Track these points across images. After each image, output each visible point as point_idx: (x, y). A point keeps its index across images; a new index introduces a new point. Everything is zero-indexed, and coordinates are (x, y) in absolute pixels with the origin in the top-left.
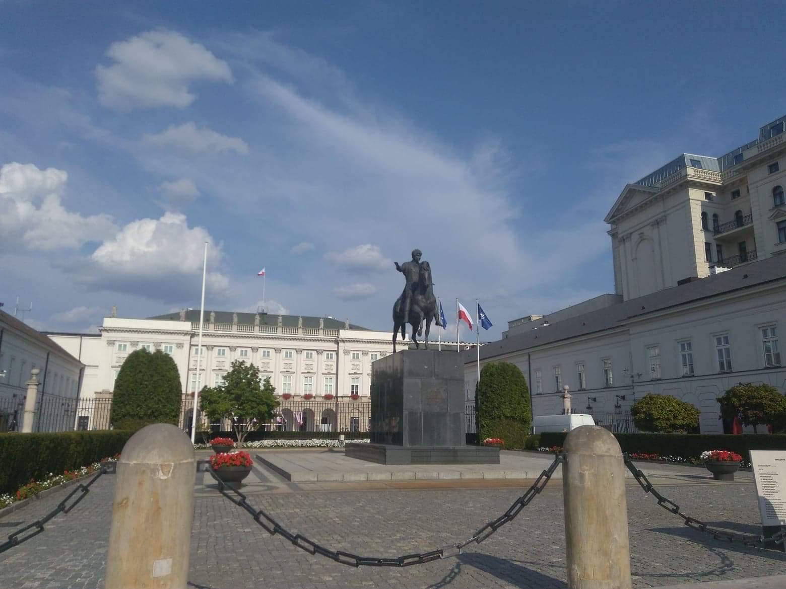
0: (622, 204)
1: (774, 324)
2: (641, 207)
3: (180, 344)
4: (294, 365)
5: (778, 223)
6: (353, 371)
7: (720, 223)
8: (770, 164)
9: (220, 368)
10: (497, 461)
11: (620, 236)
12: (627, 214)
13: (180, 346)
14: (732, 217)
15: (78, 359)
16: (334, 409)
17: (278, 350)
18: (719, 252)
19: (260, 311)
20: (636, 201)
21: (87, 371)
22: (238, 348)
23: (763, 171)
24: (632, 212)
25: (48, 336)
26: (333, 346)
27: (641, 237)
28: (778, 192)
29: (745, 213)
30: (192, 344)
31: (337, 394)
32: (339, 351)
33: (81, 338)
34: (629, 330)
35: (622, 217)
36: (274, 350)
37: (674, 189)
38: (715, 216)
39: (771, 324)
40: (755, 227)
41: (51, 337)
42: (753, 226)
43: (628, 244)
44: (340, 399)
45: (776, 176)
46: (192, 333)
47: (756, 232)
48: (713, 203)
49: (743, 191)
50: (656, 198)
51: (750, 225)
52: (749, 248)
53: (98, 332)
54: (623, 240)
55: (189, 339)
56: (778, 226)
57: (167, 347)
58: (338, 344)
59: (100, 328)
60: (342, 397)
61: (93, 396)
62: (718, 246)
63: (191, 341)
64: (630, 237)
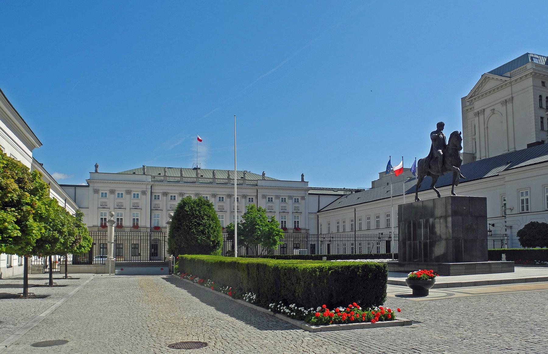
0: (478, 88)
10: (513, 271)
11: (476, 111)
13: (144, 193)
43: (481, 117)
50: (506, 85)
57: (135, 194)
63: (151, 190)
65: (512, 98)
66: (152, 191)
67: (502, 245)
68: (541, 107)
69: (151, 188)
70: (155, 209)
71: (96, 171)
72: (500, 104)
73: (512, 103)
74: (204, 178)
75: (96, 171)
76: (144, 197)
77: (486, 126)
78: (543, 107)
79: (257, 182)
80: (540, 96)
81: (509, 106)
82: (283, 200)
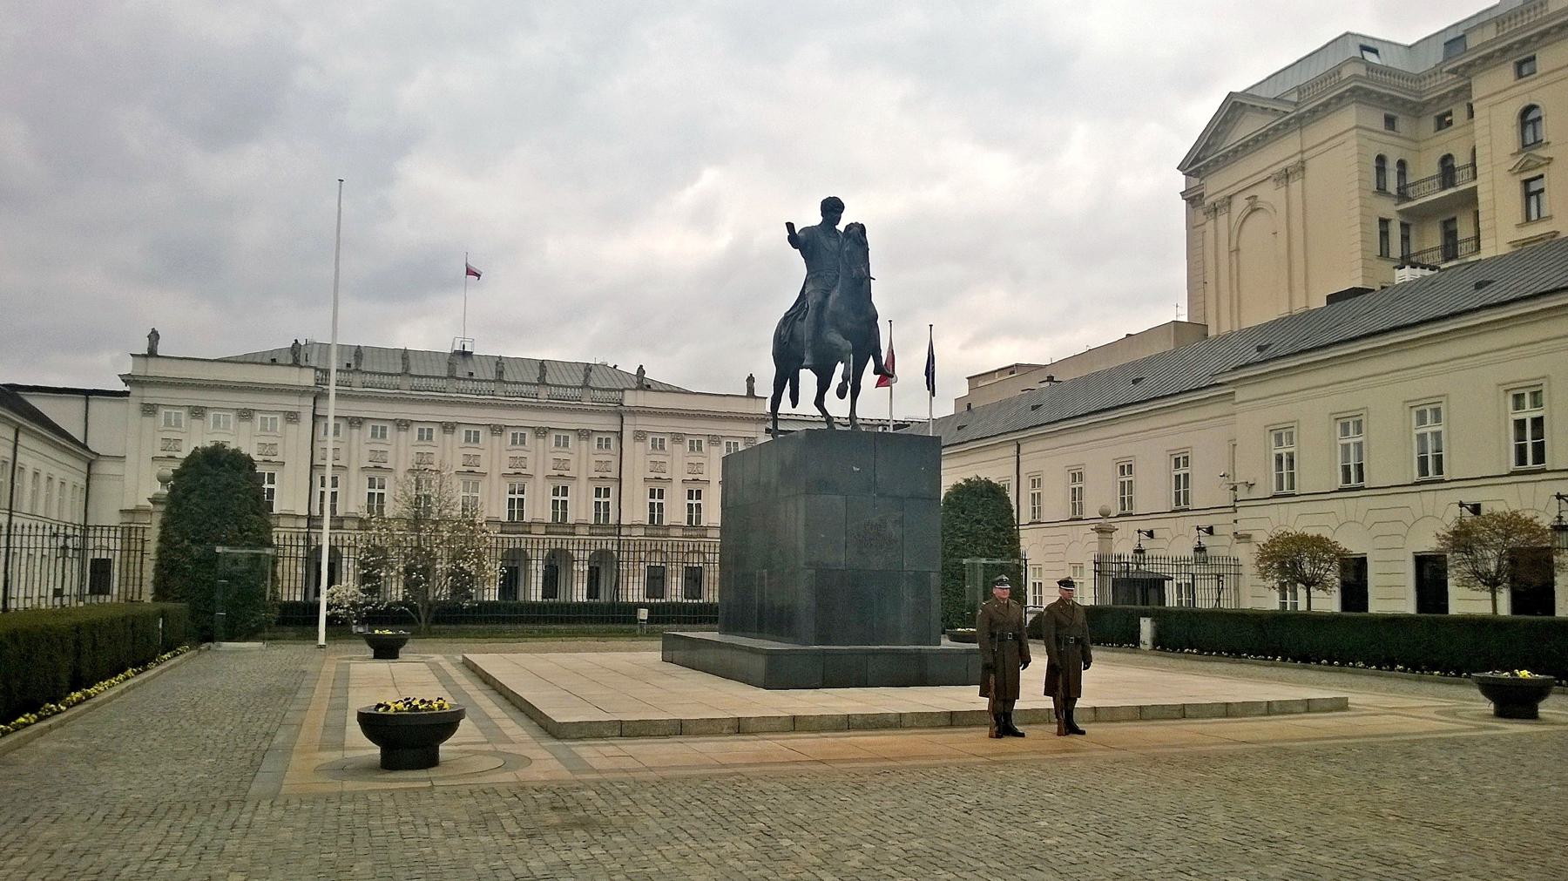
1: (1537, 382)
2: (1256, 140)
3: (290, 412)
4: (530, 463)
5: (1527, 182)
6: (653, 475)
7: (1410, 180)
9: (377, 464)
11: (1207, 202)
12: (1225, 156)
13: (292, 417)
14: (1434, 169)
15: (80, 438)
17: (497, 430)
18: (1405, 238)
19: (458, 348)
20: (1248, 127)
21: (104, 468)
22: (414, 424)
24: (1235, 151)
26: (610, 423)
27: (1250, 204)
28: (1531, 116)
29: (1461, 160)
30: (317, 413)
31: (620, 521)
32: (624, 432)
33: (87, 399)
34: (1234, 392)
35: (1216, 161)
36: (489, 432)
37: (1326, 105)
38: (1402, 164)
39: (1533, 383)
42: (1476, 187)
44: (624, 532)
45: (1530, 84)
46: (316, 390)
48: (1399, 137)
49: (1459, 114)
50: (1287, 124)
51: (1472, 184)
52: (1464, 230)
53: (121, 387)
54: (1215, 210)
55: (312, 404)
59: (126, 378)
60: (630, 526)
61: (115, 520)
62: (1402, 225)
63: (315, 408)
64: (1230, 204)
65: (1303, 162)
67: (1219, 594)
68: (1381, 190)
69: (315, 403)
71: (152, 353)
72: (1270, 182)
73: (1303, 178)
74: (476, 380)
75: (152, 353)
76: (292, 428)
78: (1388, 190)
79: (623, 395)
80: (1381, 160)
81: (1296, 185)
82: (696, 447)
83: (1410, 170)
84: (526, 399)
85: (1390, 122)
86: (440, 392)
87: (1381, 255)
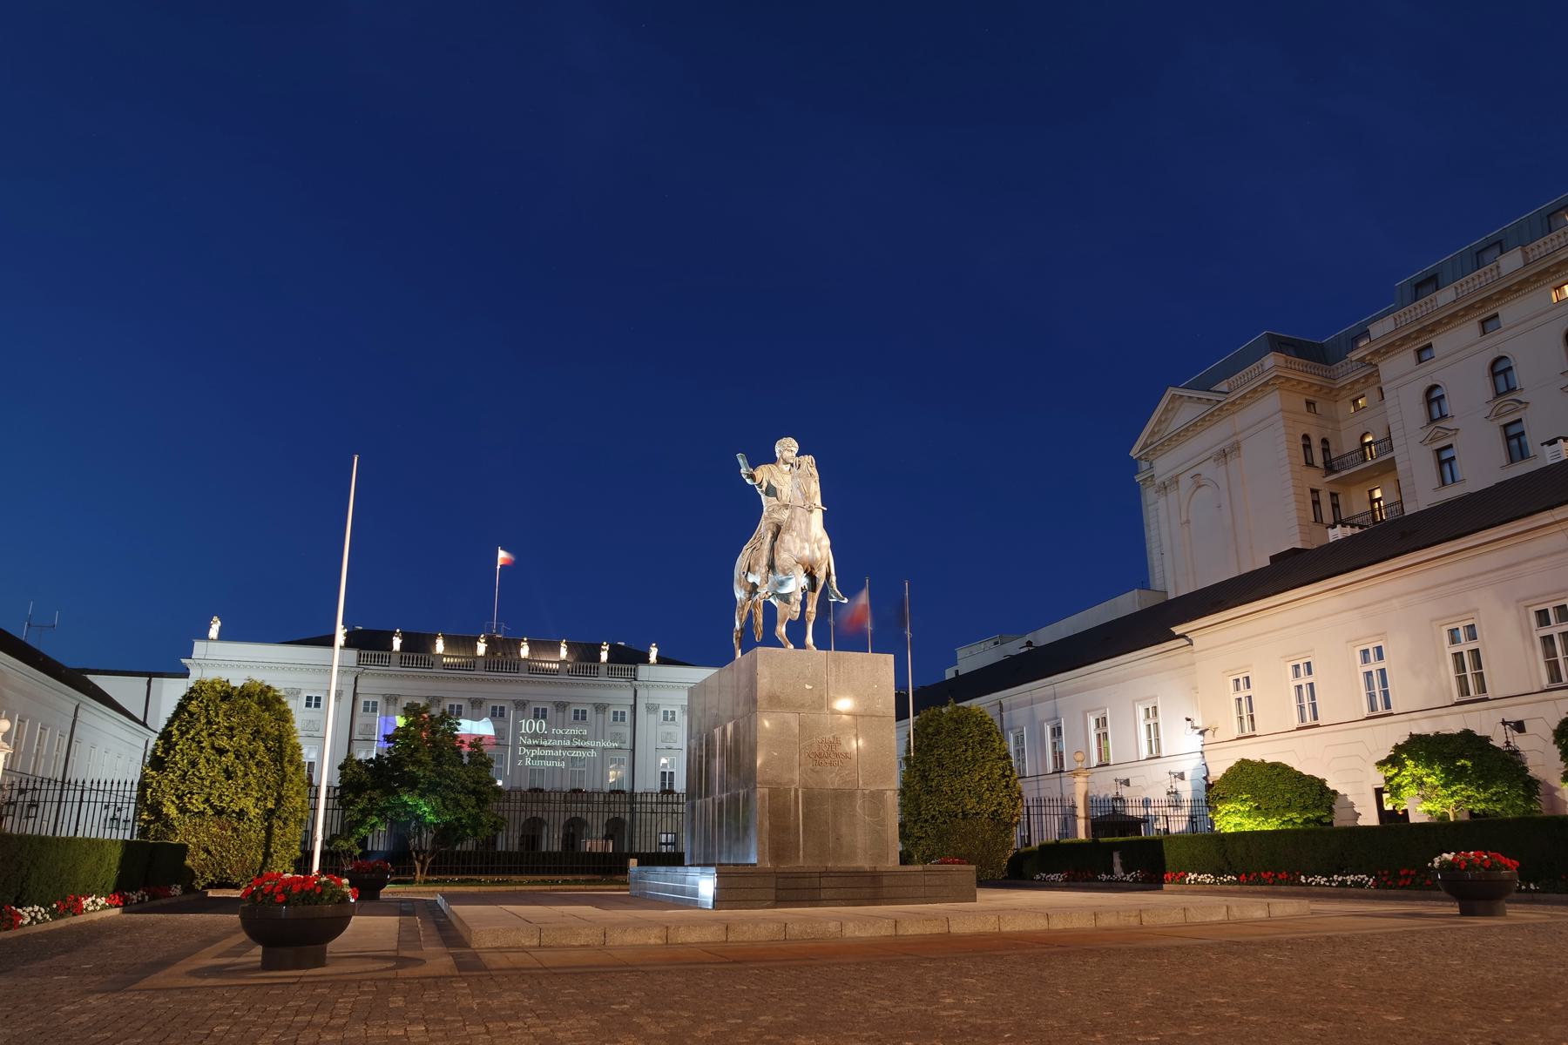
8: (1419, 346)
11: (1158, 482)
15: (142, 720)
16: (628, 818)
18: (1335, 506)
23: (1405, 359)
25: (90, 677)
31: (633, 789)
38: (1325, 441)
40: (1397, 461)
41: (90, 677)
47: (1399, 467)
50: (1221, 409)
51: (1389, 456)
56: (1439, 457)
58: (636, 691)
62: (1333, 495)
64: (1177, 482)
65: (1238, 443)
66: (358, 691)
68: (1310, 463)
70: (360, 737)
77: (1184, 519)
80: (1306, 437)
83: (1332, 446)
84: (544, 676)
85: (1309, 403)
86: (470, 670)
87: (1316, 521)
